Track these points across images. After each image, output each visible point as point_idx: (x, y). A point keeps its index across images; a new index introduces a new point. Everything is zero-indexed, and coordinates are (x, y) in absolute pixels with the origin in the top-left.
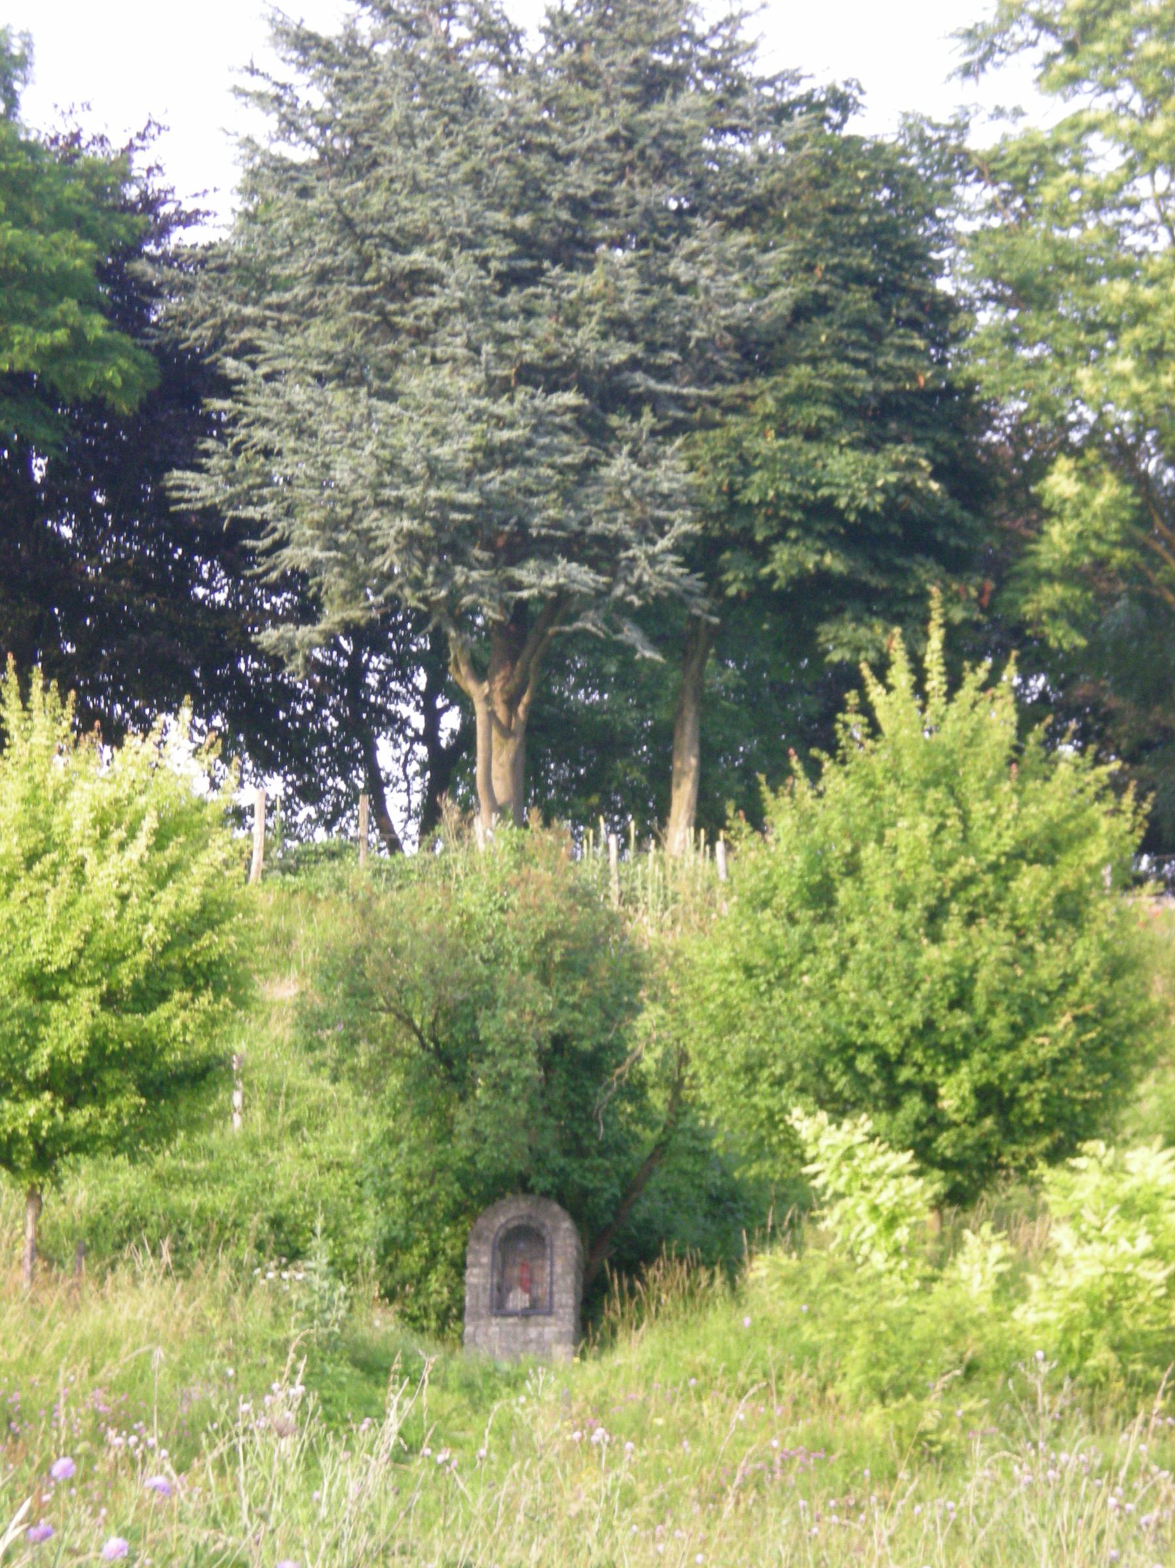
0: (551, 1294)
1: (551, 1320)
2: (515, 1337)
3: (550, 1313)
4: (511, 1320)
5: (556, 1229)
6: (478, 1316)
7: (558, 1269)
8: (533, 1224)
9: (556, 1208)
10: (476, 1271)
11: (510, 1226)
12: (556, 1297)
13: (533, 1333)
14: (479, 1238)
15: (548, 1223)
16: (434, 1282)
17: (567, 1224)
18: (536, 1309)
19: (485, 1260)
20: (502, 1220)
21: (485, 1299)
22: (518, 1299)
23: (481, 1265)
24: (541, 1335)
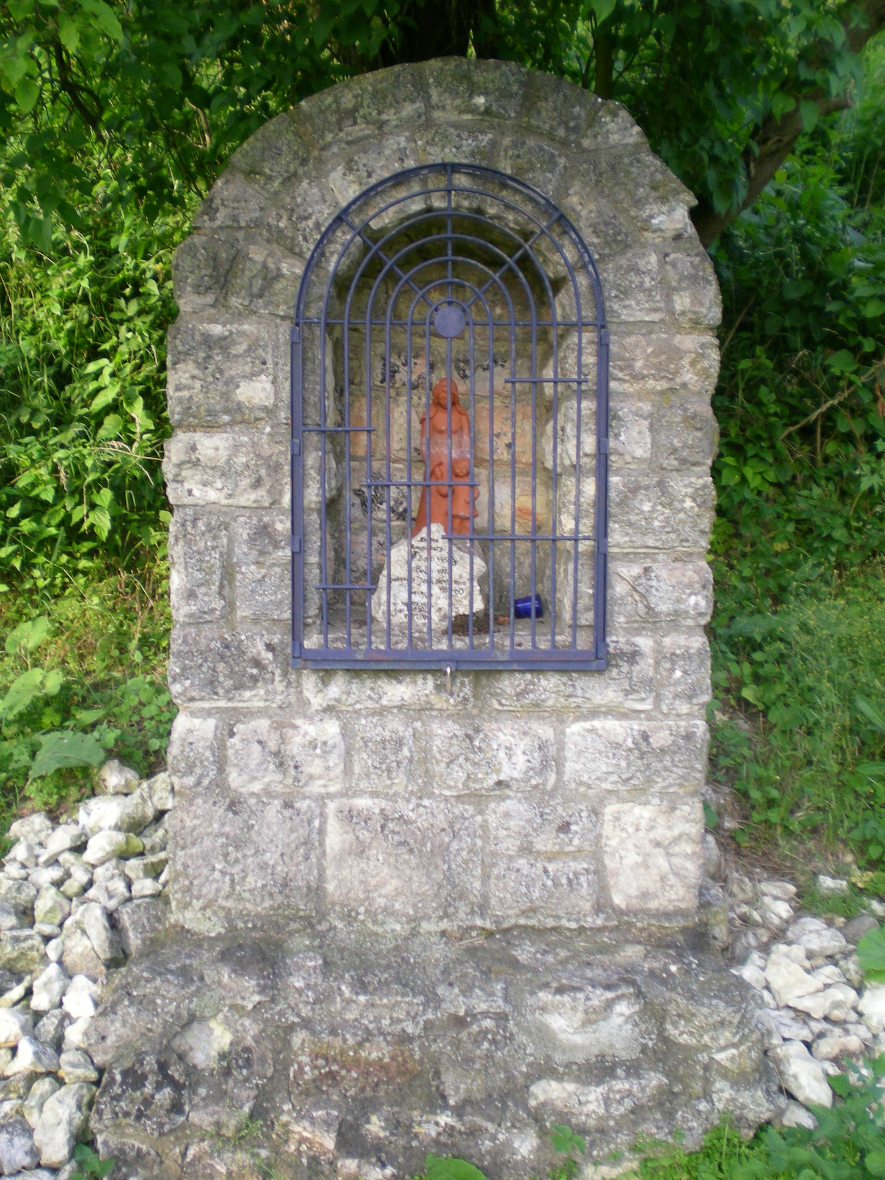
0: (601, 561)
1: (603, 691)
2: (422, 764)
3: (597, 660)
4: (398, 692)
5: (622, 240)
6: (230, 667)
7: (634, 441)
8: (505, 213)
9: (620, 130)
10: (212, 446)
11: (385, 217)
12: (624, 574)
13: (511, 748)
14: (222, 278)
15: (582, 206)
16: (104, 380)
17: (674, 216)
18: (523, 626)
19: (258, 391)
20: (344, 188)
21: (263, 585)
22: (426, 581)
23: (241, 417)
24: (550, 758)
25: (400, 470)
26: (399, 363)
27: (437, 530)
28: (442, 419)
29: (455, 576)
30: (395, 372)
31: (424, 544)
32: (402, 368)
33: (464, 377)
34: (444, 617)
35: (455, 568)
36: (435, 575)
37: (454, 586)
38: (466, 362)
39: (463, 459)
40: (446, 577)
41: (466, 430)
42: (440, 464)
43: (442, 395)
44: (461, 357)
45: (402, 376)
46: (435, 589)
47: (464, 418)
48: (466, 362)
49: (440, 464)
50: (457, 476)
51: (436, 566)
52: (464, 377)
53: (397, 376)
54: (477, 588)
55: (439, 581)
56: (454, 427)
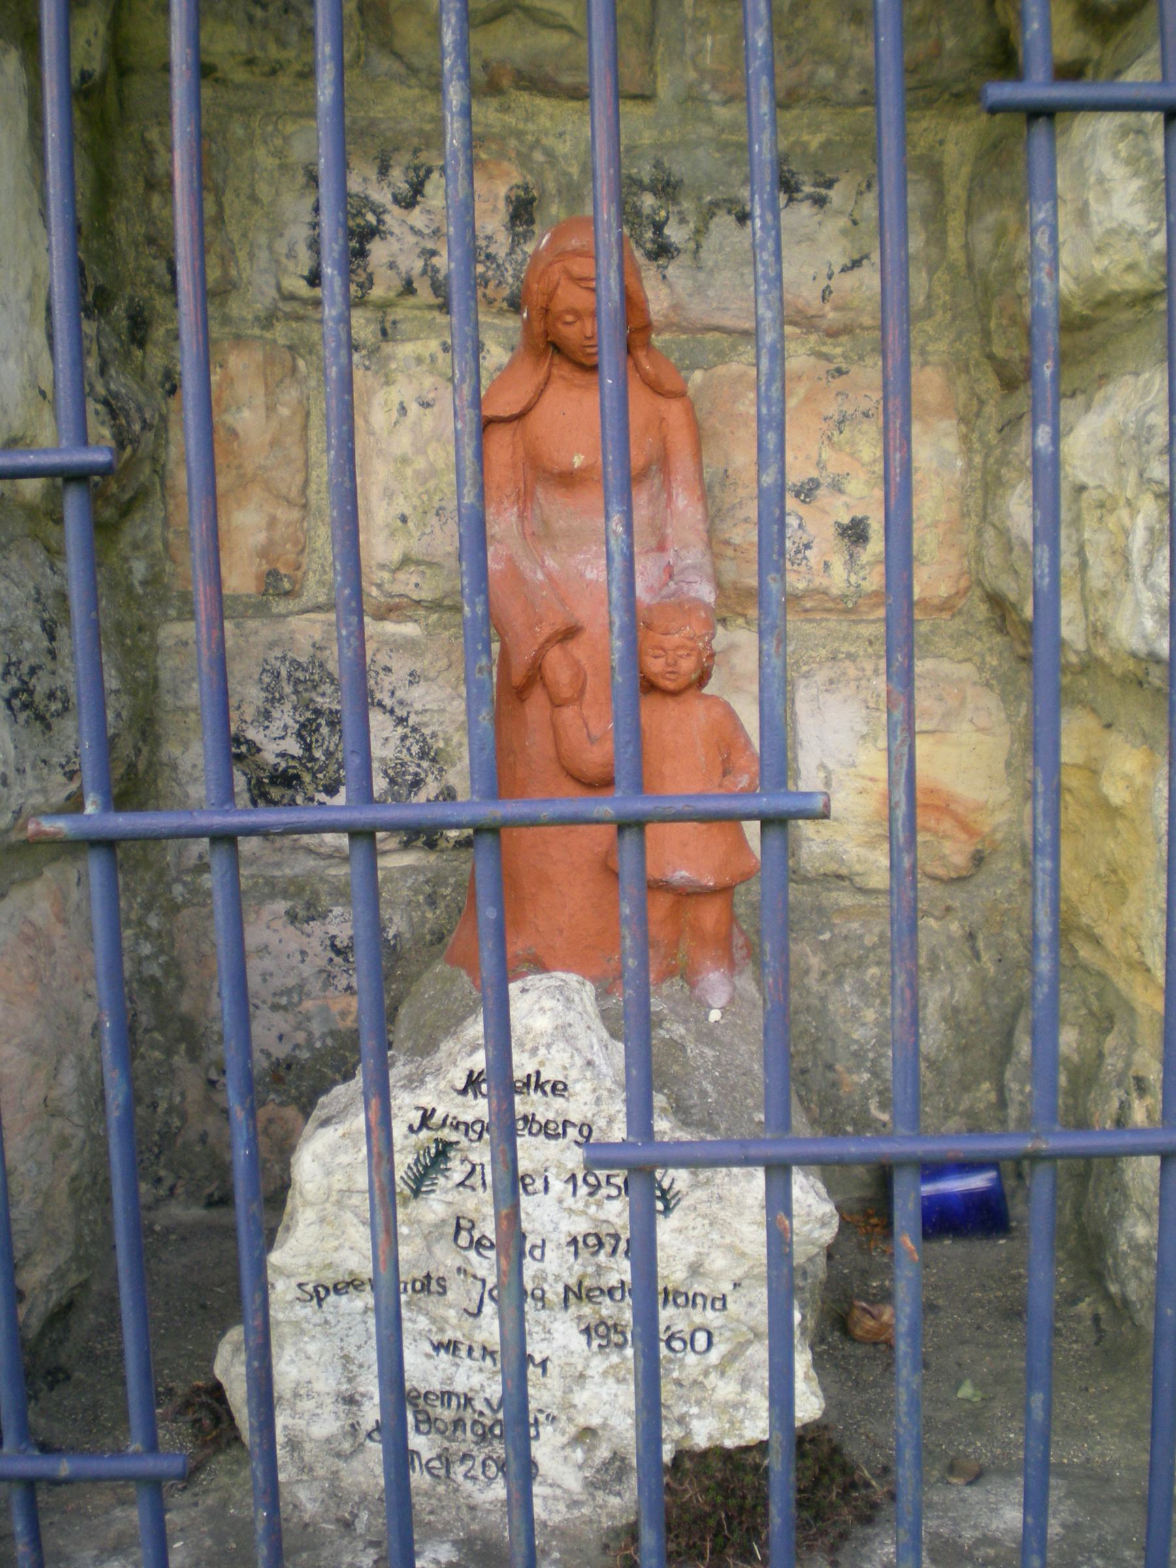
25: (409, 646)
26: (381, 196)
27: (556, 1022)
28: (572, 422)
29: (671, 1270)
30: (371, 233)
31: (478, 1108)
32: (394, 217)
33: (662, 251)
34: (610, 1473)
35: (665, 1229)
36: (551, 1267)
37: (666, 1315)
38: (667, 188)
39: (685, 607)
40: (621, 1270)
41: (682, 463)
42: (570, 633)
43: (570, 297)
44: (645, 172)
45: (394, 252)
46: (557, 1337)
47: (674, 411)
48: (667, 188)
49: (570, 633)
50: (649, 686)
51: (550, 1215)
52: (662, 251)
53: (378, 251)
54: (802, 1361)
55: (576, 1293)
56: (638, 459)
